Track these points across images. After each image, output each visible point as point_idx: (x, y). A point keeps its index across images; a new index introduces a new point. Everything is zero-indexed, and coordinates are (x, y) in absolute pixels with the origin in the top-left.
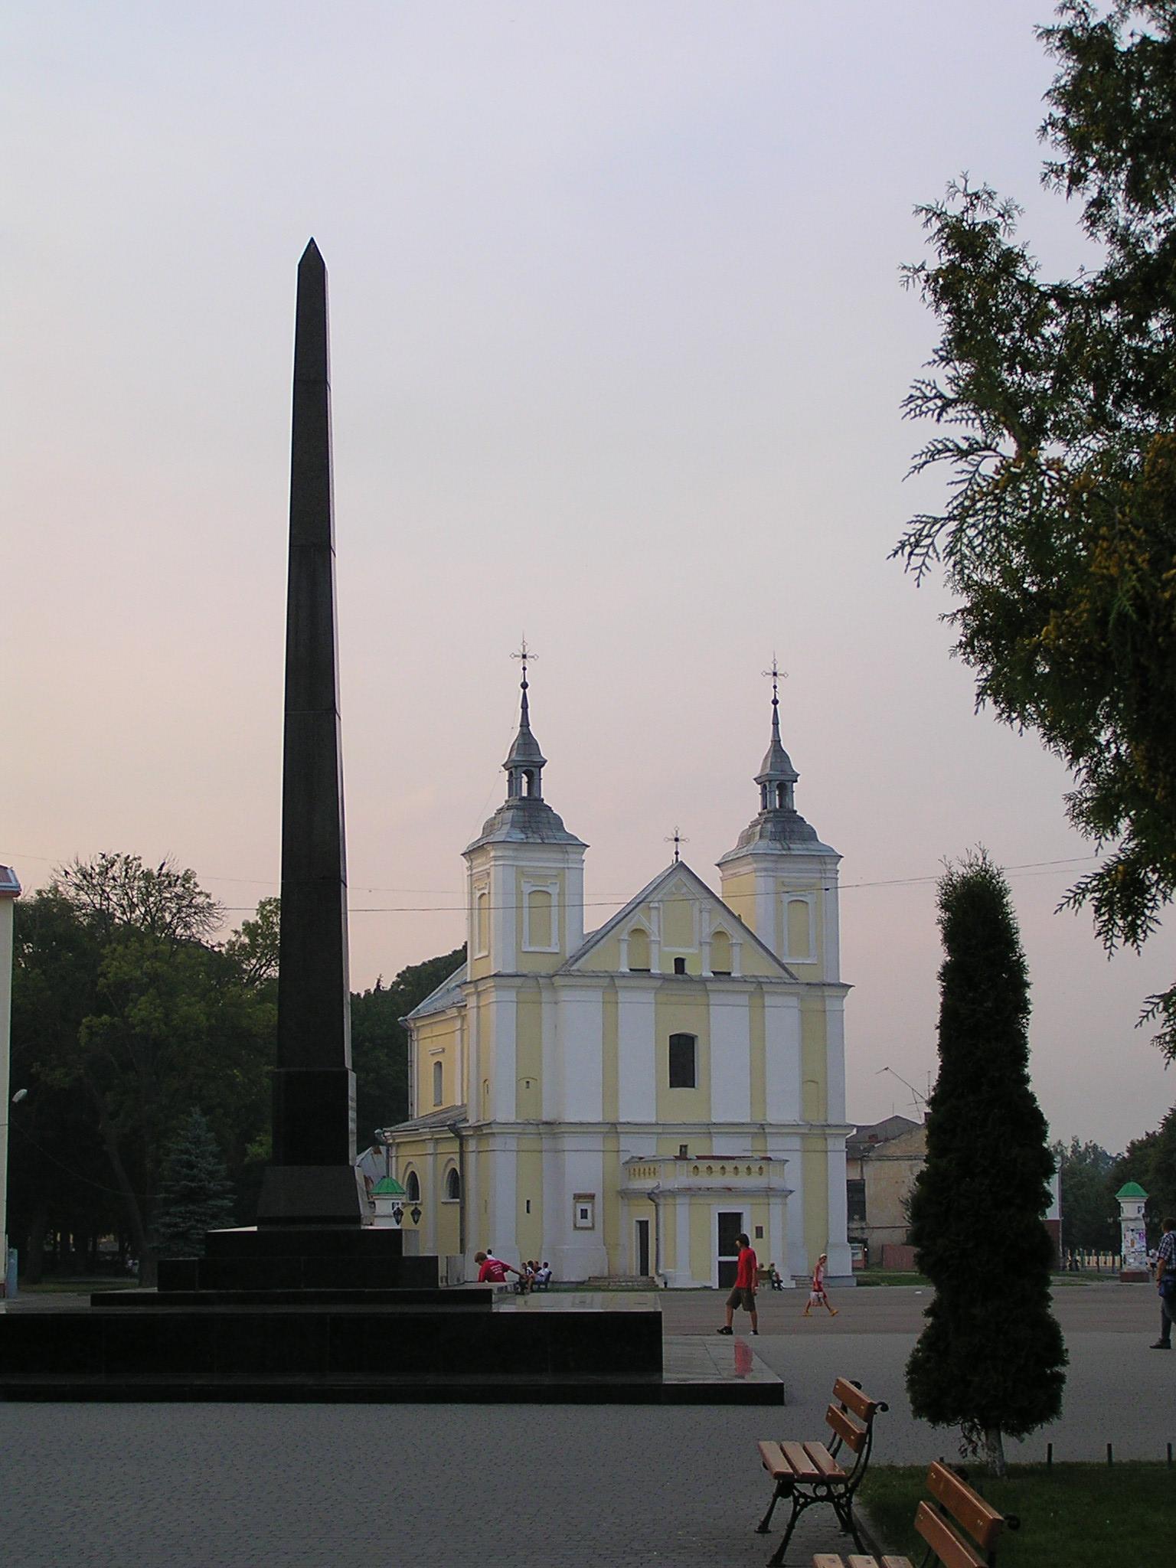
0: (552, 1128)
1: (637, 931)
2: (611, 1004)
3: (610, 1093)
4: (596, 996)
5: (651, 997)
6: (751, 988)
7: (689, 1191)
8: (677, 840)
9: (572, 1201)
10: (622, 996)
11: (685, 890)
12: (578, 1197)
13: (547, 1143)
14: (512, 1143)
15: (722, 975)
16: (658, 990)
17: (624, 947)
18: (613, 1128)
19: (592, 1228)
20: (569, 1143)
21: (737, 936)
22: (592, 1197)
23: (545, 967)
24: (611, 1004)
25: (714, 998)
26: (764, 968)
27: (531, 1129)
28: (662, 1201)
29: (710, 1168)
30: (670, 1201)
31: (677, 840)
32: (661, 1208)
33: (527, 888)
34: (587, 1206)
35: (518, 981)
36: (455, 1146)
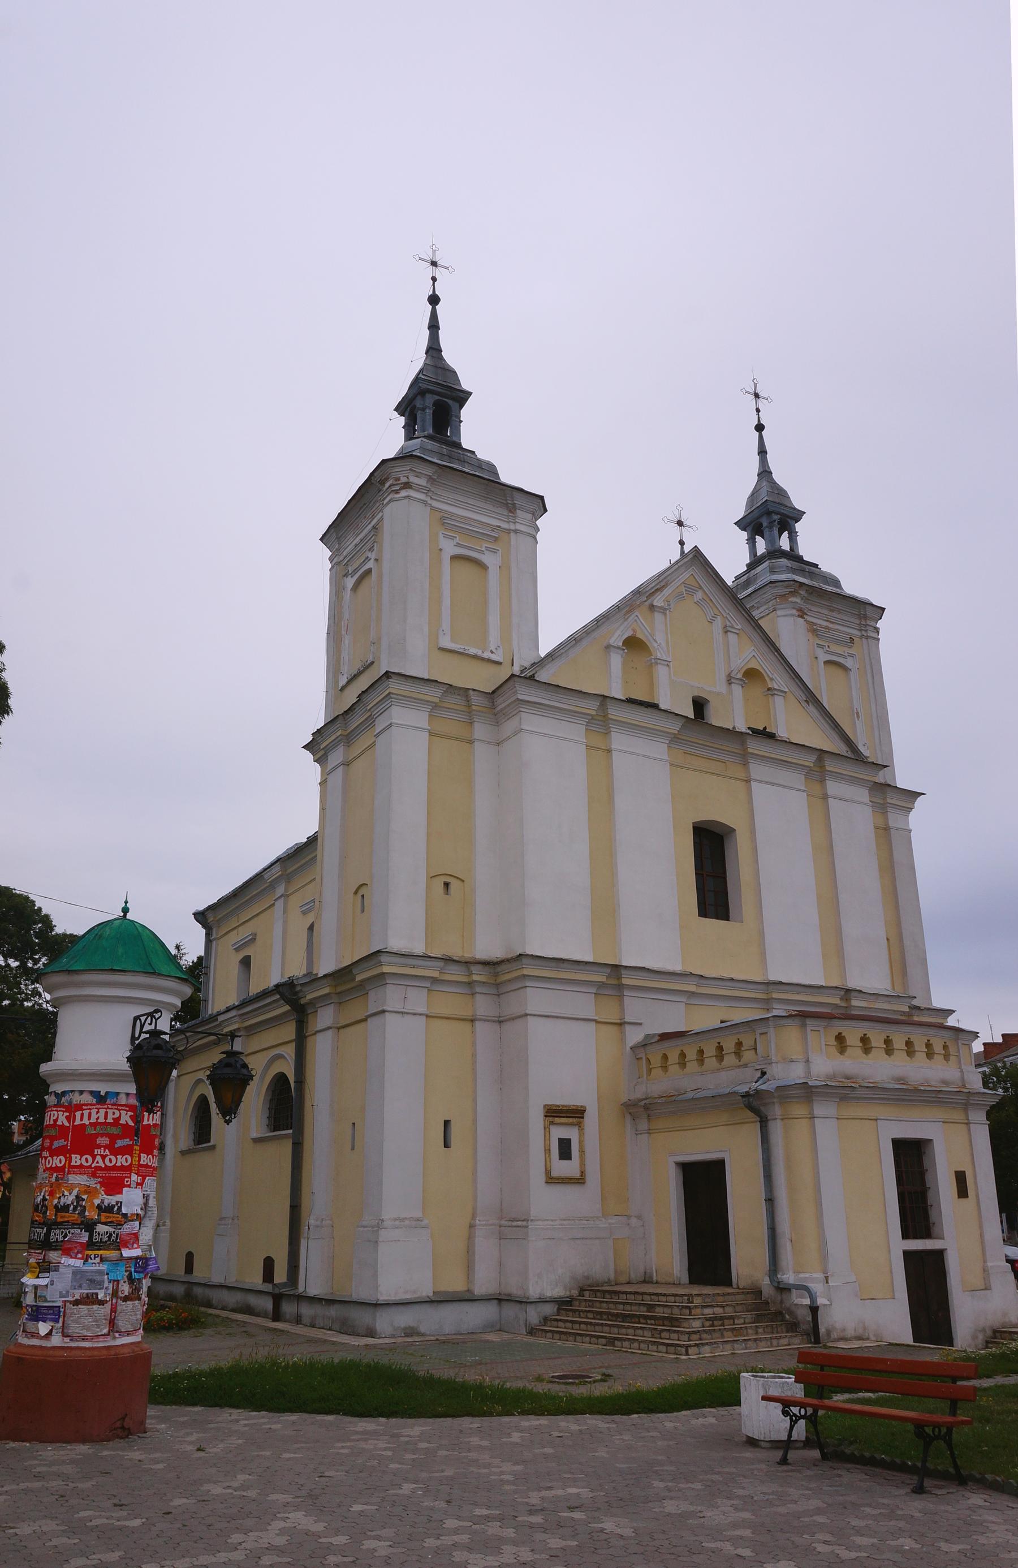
0: (501, 975)
1: (634, 644)
2: (601, 753)
3: (605, 909)
4: (576, 731)
5: (659, 749)
6: (810, 760)
7: (845, 1092)
8: (680, 523)
9: (537, 1119)
10: (619, 740)
11: (699, 595)
12: (554, 1113)
13: (483, 1005)
14: (418, 1000)
15: (766, 735)
16: (674, 740)
17: (616, 660)
18: (614, 979)
19: (580, 1180)
20: (537, 999)
21: (779, 680)
22: (576, 1114)
23: (483, 679)
24: (601, 753)
25: (757, 770)
26: (820, 738)
27: (455, 974)
28: (777, 1110)
29: (865, 1040)
30: (799, 1110)
31: (680, 523)
32: (776, 1128)
33: (449, 548)
34: (572, 1134)
35: (433, 694)
36: (288, 1031)
